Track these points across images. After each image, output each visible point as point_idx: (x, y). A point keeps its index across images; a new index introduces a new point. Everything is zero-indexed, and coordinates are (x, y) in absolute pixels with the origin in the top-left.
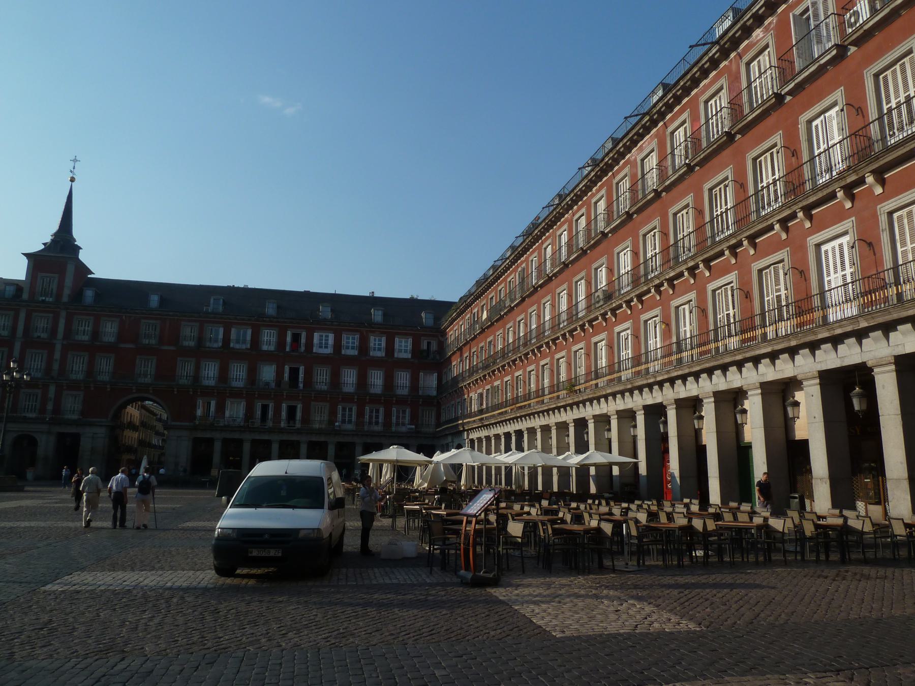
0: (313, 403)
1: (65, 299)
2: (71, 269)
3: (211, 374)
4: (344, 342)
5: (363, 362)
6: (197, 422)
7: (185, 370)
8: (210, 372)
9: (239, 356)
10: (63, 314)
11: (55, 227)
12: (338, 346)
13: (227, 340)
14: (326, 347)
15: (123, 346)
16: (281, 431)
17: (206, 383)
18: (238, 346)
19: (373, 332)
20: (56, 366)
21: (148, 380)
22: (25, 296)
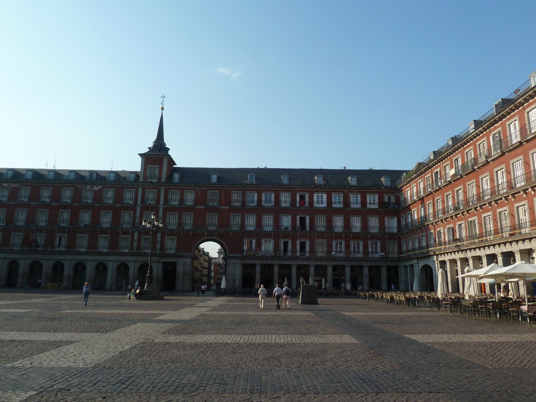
0: (316, 240)
1: (163, 180)
2: (165, 161)
3: (251, 223)
4: (333, 200)
5: (347, 212)
6: (245, 254)
7: (235, 221)
8: (251, 222)
9: (268, 211)
10: (163, 189)
11: (154, 137)
12: (329, 202)
13: (259, 201)
14: (322, 203)
15: (198, 207)
16: (297, 258)
17: (249, 228)
18: (266, 205)
19: (351, 192)
21: (213, 228)
22: (141, 180)
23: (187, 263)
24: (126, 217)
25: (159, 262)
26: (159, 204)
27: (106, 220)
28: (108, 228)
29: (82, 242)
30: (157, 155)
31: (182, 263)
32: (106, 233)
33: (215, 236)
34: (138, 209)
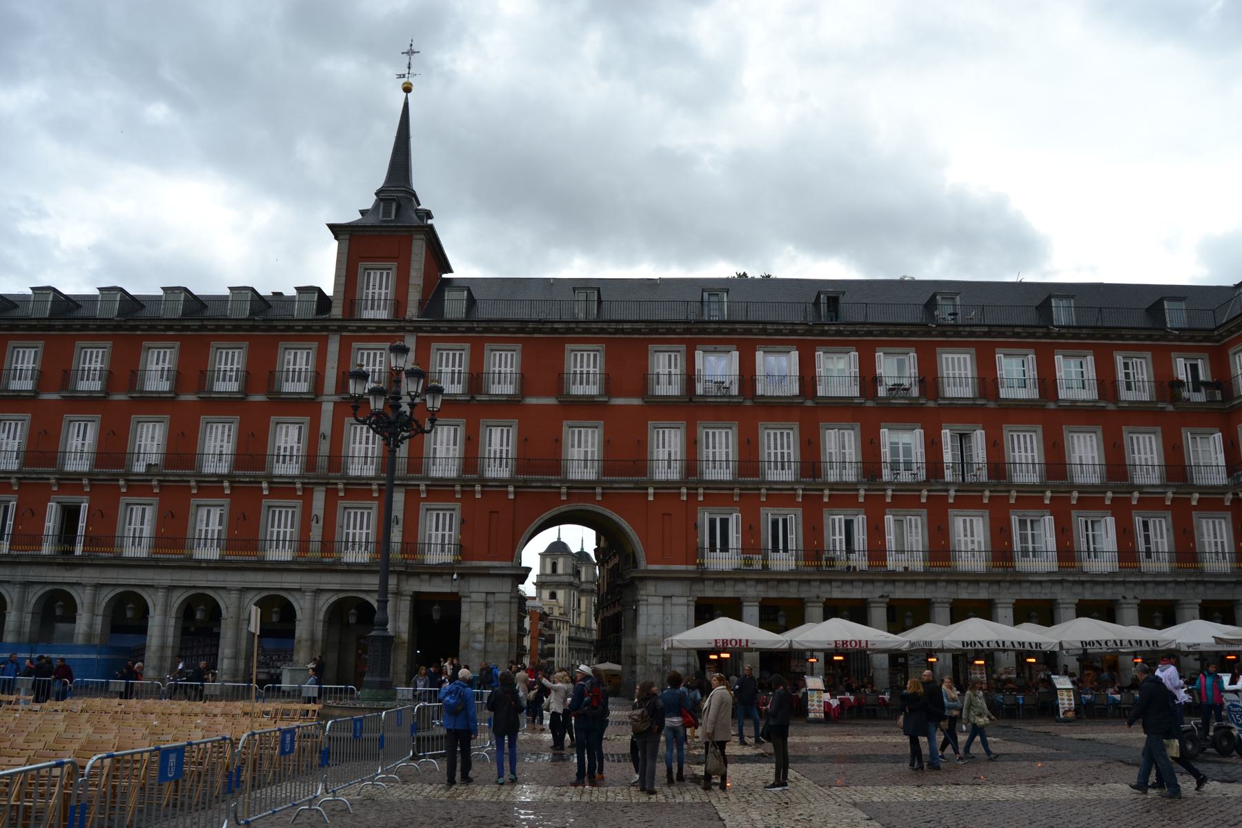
1: (412, 311)
2: (419, 249)
7: (666, 448)
9: (777, 409)
17: (711, 474)
22: (337, 311)
23: (498, 597)
24: (288, 438)
27: (218, 445)
28: (222, 477)
29: (138, 526)
30: (391, 232)
31: (482, 597)
32: (218, 492)
33: (599, 503)
34: (328, 408)
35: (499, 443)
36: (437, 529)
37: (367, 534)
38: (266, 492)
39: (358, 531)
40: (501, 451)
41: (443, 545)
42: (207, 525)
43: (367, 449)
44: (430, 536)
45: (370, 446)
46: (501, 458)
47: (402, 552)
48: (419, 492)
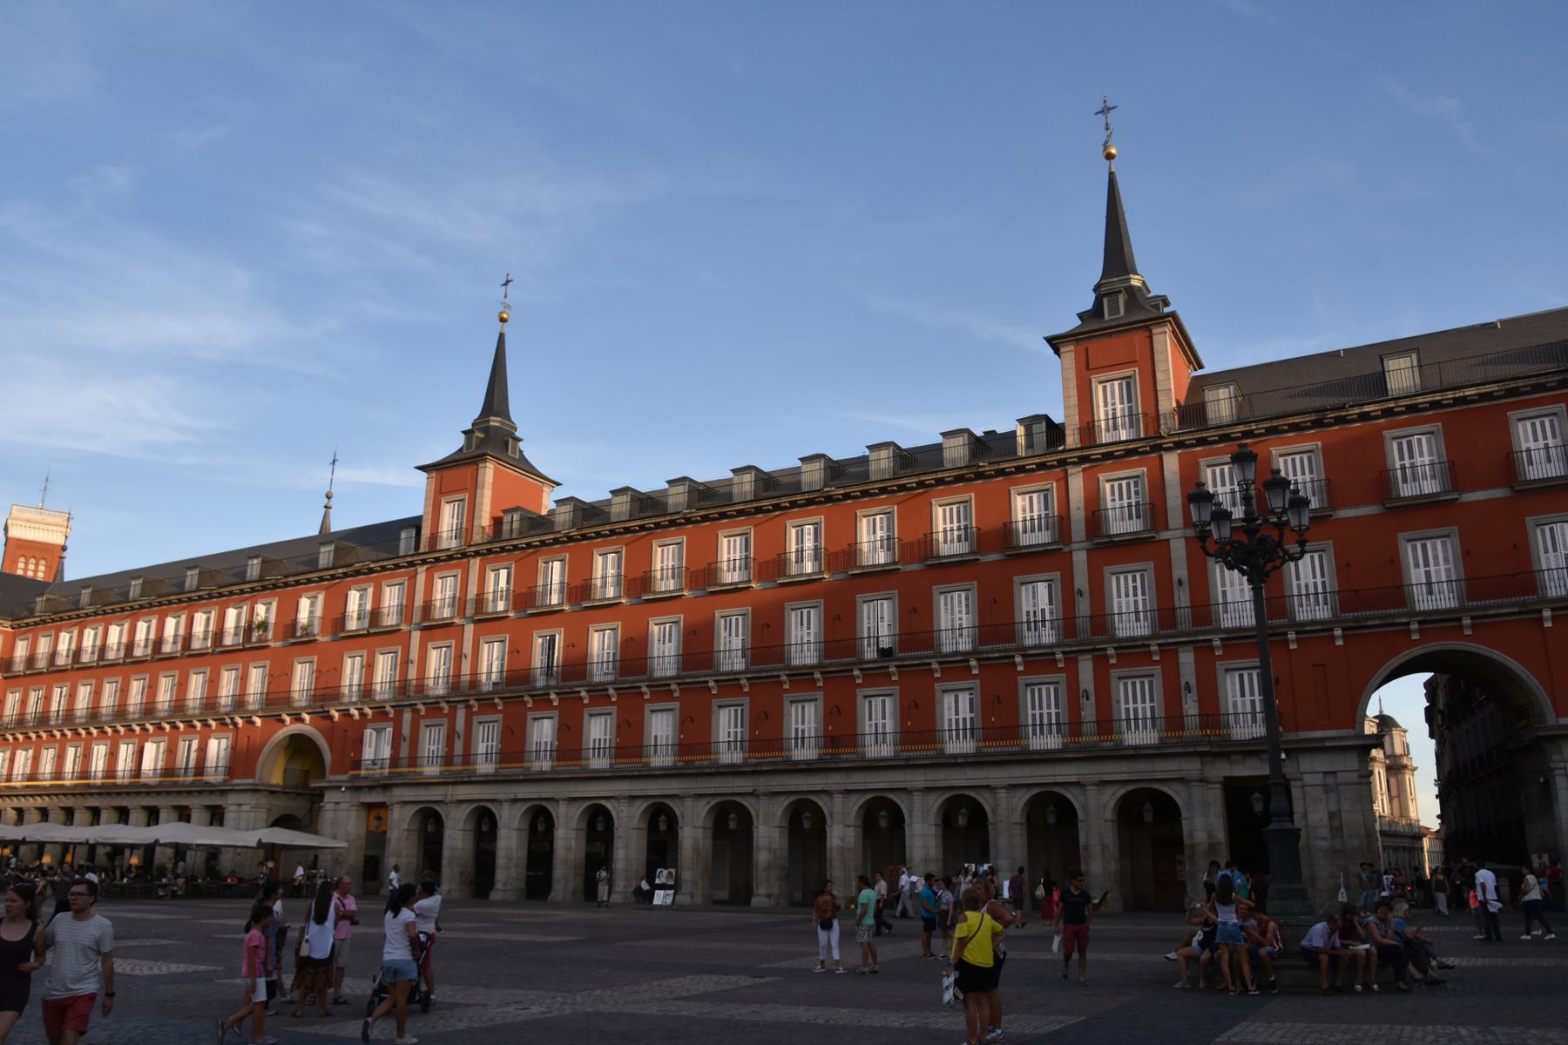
20: (1182, 598)
22: (1072, 440)
23: (1341, 777)
24: (1036, 599)
25: (1203, 780)
26: (1167, 528)
29: (879, 718)
31: (1319, 779)
34: (1080, 558)
35: (1309, 578)
36: (1243, 695)
37: (1152, 708)
38: (1020, 668)
39: (1137, 705)
40: (1315, 584)
41: (1254, 713)
42: (957, 713)
43: (1136, 602)
44: (1235, 704)
45: (1140, 598)
46: (1316, 594)
47: (1203, 726)
48: (1212, 649)
